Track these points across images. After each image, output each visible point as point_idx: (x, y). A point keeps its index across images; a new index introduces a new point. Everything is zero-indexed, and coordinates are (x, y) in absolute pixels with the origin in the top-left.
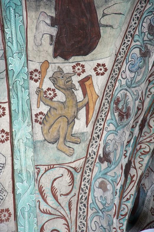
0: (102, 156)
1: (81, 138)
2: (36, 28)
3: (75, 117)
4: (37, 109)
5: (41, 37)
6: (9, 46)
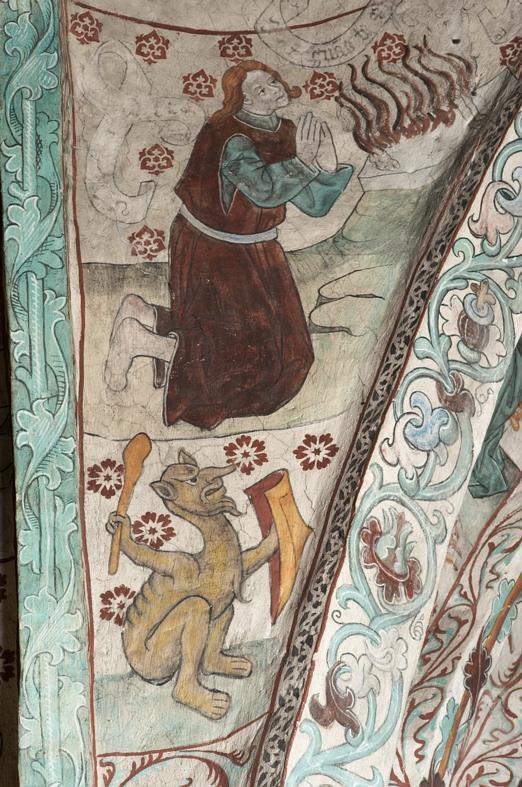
0: (322, 701)
1: (252, 659)
2: (112, 341)
3: (235, 597)
4: (111, 576)
5: (125, 365)
6: (21, 381)
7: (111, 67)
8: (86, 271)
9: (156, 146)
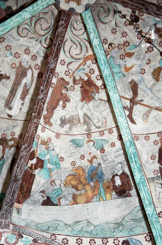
5: (159, 194)
7: (142, 143)
8: (148, 180)
9: (153, 155)
